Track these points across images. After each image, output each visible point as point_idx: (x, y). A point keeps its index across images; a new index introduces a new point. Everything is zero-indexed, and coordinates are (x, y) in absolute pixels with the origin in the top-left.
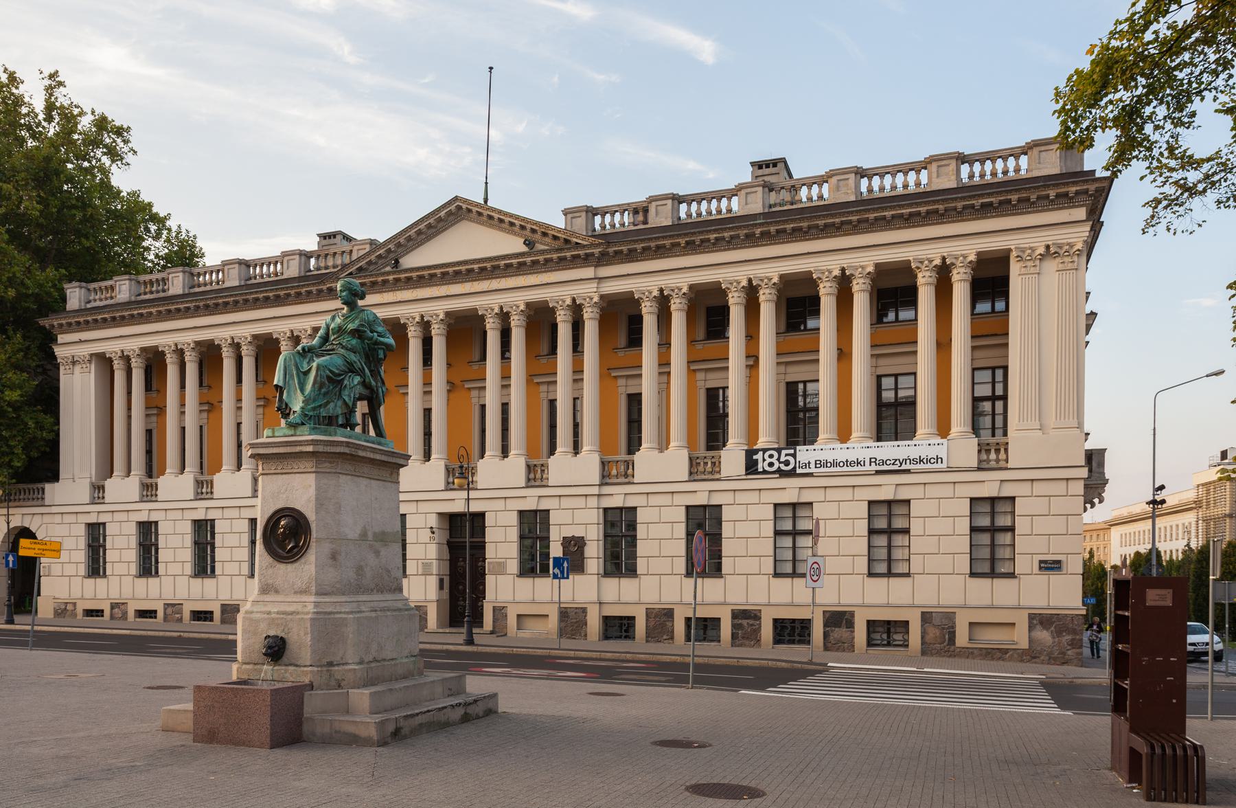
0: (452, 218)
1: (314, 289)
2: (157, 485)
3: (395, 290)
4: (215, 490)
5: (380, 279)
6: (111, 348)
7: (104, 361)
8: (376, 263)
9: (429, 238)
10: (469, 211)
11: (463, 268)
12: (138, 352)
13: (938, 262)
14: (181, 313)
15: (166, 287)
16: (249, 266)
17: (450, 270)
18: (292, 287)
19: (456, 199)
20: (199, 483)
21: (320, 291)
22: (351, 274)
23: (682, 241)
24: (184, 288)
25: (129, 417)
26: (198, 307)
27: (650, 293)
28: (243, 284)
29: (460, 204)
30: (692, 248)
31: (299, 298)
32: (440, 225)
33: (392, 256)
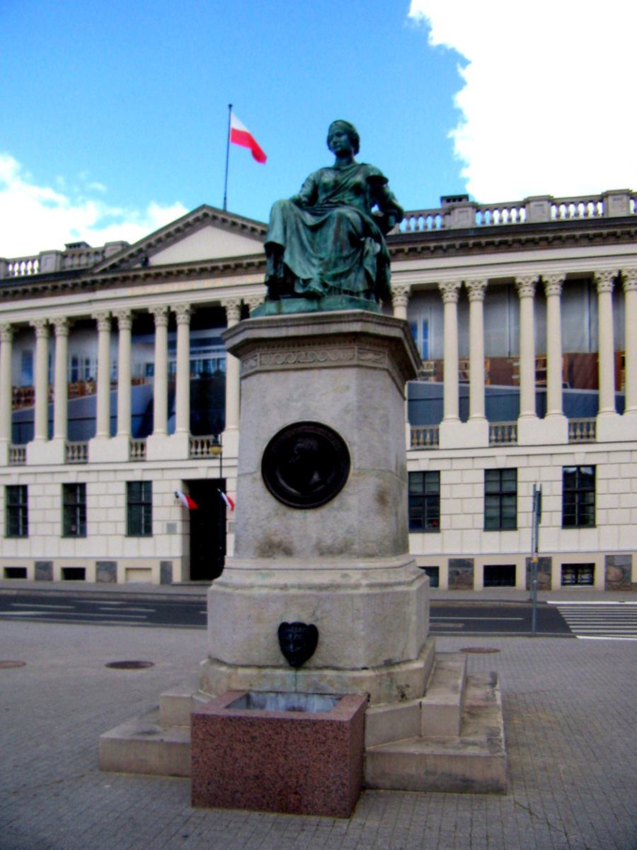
0: (198, 223)
8: (127, 261)
9: (176, 240)
10: (215, 218)
11: (209, 266)
13: (616, 274)
19: (204, 207)
23: (406, 248)
29: (208, 212)
31: (55, 291)
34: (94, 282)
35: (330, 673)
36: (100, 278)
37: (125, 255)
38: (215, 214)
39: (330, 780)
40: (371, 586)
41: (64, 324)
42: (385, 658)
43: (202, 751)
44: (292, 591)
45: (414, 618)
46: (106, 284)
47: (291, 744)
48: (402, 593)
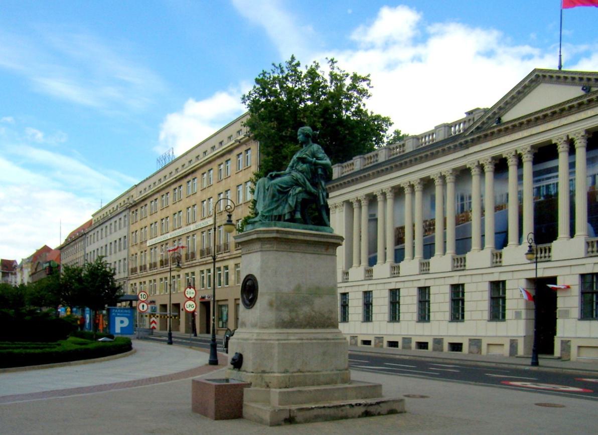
0: (533, 84)
3: (499, 137)
5: (489, 132)
6: (351, 197)
7: (349, 204)
8: (487, 123)
9: (519, 100)
10: (544, 76)
19: (535, 70)
22: (472, 132)
24: (386, 157)
31: (445, 153)
32: (526, 91)
33: (497, 116)
34: (466, 142)
35: (245, 373)
36: (469, 138)
37: (484, 119)
38: (544, 74)
40: (256, 340)
41: (391, 191)
42: (263, 369)
44: (240, 341)
45: (276, 355)
46: (474, 142)
48: (270, 343)
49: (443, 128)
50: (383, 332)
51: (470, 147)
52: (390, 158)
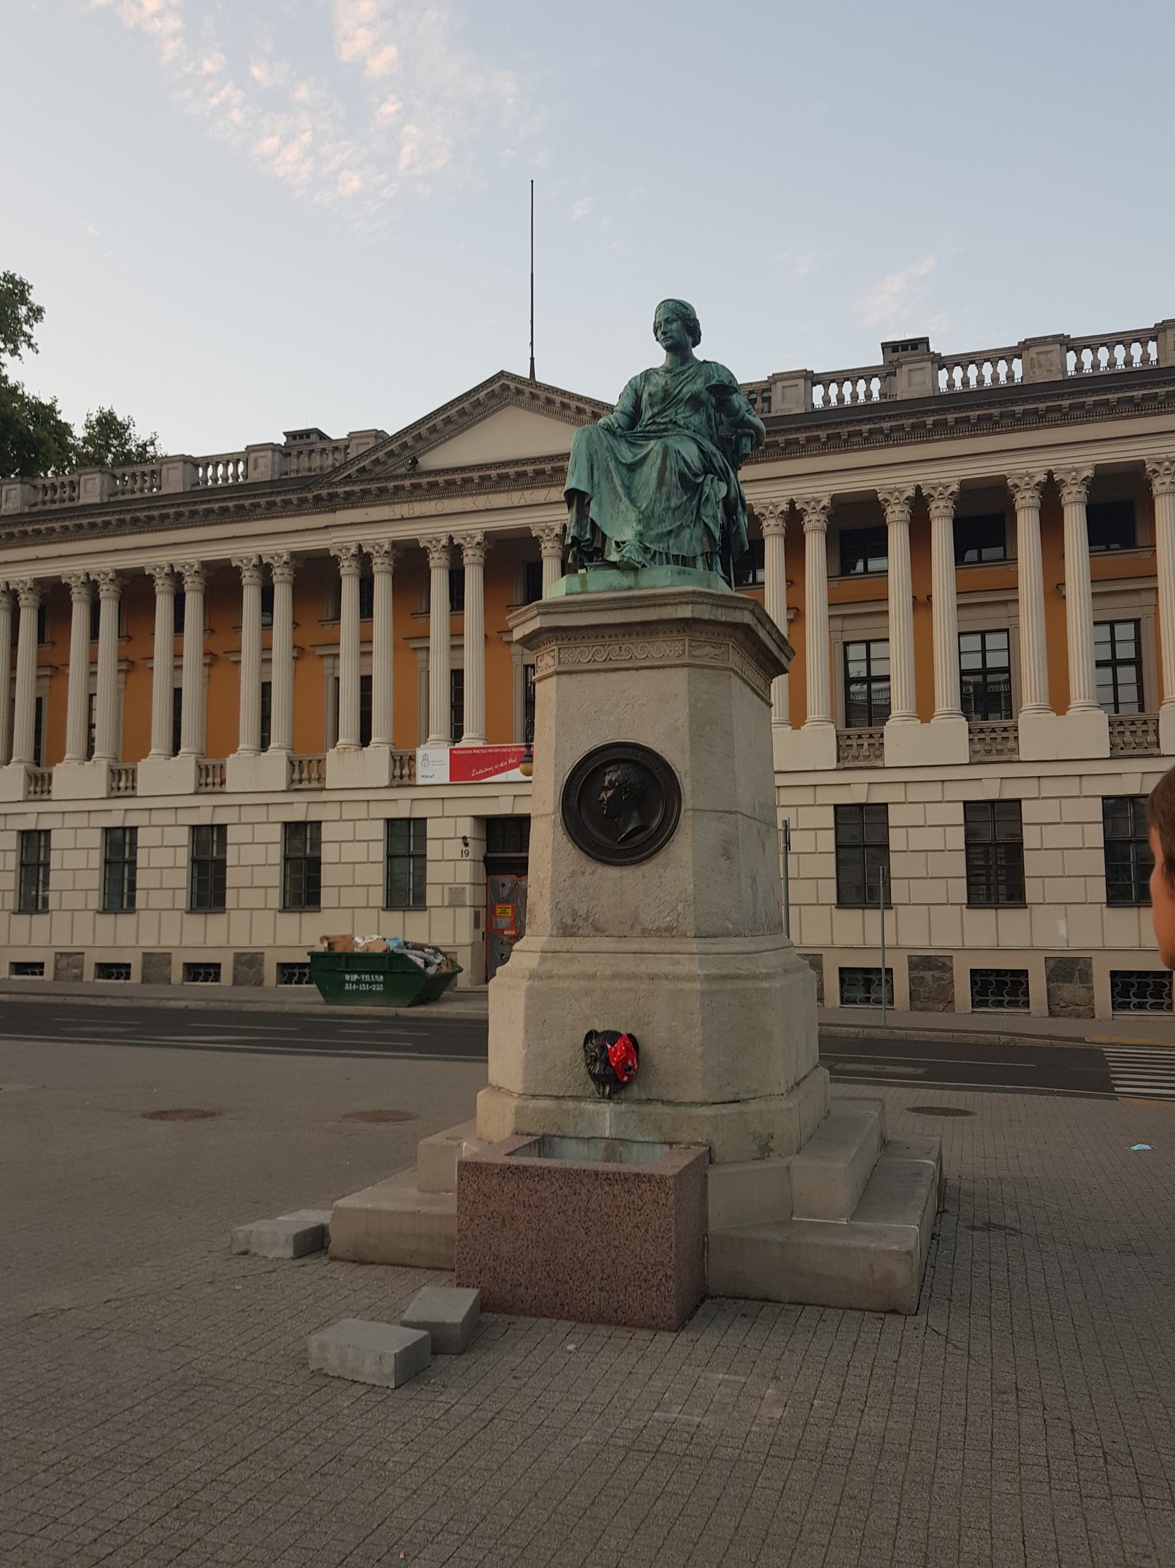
0: (494, 401)
1: (294, 497)
2: (50, 776)
4: (139, 784)
5: (391, 485)
8: (384, 463)
10: (519, 392)
12: (30, 584)
14: (96, 531)
15: (75, 495)
16: (197, 466)
17: (493, 473)
18: (262, 494)
19: (502, 374)
20: (115, 774)
21: (303, 501)
22: (349, 476)
23: (823, 434)
25: (13, 680)
26: (122, 522)
27: (776, 507)
28: (188, 490)
29: (507, 382)
30: (836, 444)
32: (477, 412)
36: (341, 490)
39: (649, 1269)
43: (472, 1219)
46: (350, 501)
47: (594, 1211)
49: (270, 453)
50: (170, 940)
51: (340, 509)
52: (113, 499)
